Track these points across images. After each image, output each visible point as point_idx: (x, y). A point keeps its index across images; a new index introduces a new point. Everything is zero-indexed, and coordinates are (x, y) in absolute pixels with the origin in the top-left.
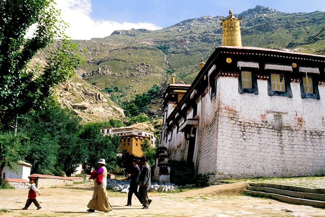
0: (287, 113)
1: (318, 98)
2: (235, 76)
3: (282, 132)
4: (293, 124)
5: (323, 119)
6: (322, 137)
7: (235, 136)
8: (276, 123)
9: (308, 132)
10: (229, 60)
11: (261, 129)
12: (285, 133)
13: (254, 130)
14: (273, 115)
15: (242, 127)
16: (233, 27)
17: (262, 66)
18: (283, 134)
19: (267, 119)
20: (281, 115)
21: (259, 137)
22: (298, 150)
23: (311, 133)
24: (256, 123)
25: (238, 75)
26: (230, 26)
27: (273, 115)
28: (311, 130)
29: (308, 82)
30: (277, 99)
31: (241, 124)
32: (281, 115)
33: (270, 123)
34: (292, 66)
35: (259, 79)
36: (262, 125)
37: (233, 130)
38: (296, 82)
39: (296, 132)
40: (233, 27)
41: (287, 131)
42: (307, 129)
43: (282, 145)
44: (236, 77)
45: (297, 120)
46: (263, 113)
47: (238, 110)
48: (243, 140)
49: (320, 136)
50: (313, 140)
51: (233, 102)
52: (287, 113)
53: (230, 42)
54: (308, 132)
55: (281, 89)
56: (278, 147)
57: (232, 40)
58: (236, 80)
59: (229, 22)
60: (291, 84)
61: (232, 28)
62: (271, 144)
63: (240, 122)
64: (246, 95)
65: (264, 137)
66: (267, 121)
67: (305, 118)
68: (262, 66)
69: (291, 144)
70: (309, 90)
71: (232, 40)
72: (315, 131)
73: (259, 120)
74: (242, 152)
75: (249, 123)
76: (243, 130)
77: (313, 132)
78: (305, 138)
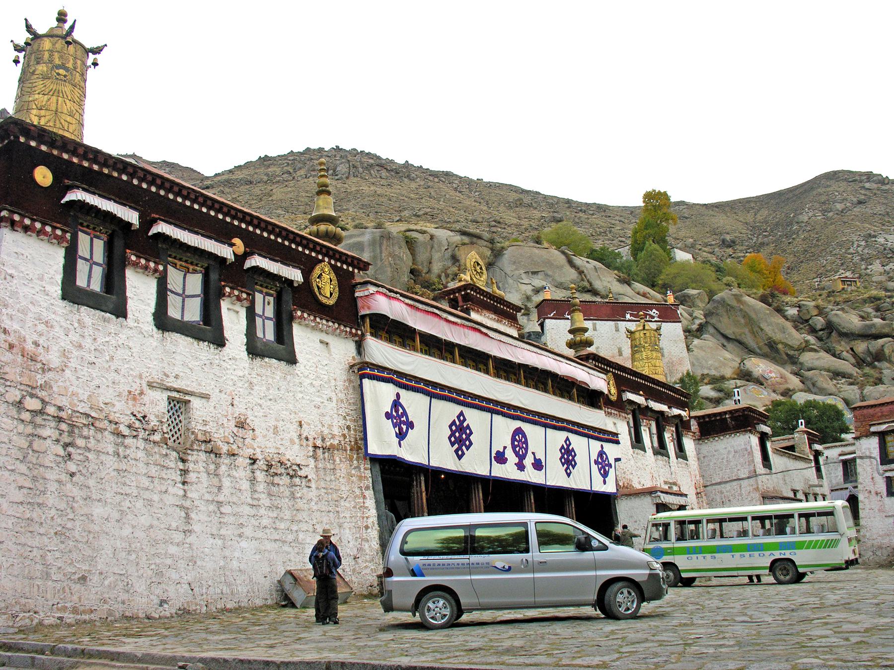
0: (205, 397)
1: (292, 360)
2: (56, 237)
3: (190, 458)
4: (221, 434)
5: (301, 426)
6: (297, 480)
7: (37, 459)
8: (177, 424)
9: (261, 464)
10: (43, 176)
11: (128, 441)
12: (198, 460)
13: (108, 442)
14: (165, 395)
15: (64, 426)
16: (67, 69)
17: (147, 222)
18: (191, 466)
19: (146, 410)
20: (187, 402)
21: (118, 470)
22: (232, 519)
23: (270, 466)
24: (111, 418)
25: (68, 236)
26: (57, 61)
27: (165, 395)
28: (269, 459)
29: (265, 305)
30: (182, 343)
31: (63, 414)
32: (187, 402)
33: (154, 422)
34: (232, 245)
35: (135, 265)
36: (129, 426)
37: (33, 435)
38: (239, 299)
39: (227, 460)
40: (67, 69)
41: (203, 456)
42: (259, 456)
43: (188, 504)
44: (60, 240)
45: (232, 423)
46: (136, 389)
47: (53, 358)
48: (64, 477)
49: (292, 477)
50: (274, 489)
51: (41, 327)
52: (205, 397)
53: (47, 118)
54: (261, 464)
55: (193, 313)
56: (178, 510)
57: (57, 111)
58: (58, 256)
59: (57, 46)
60: (222, 302)
61: (61, 71)
62: (156, 498)
63: (60, 409)
64: (87, 315)
65: (134, 470)
66: (144, 417)
67: (254, 420)
68: (147, 222)
69: (213, 501)
70: (267, 332)
71: (57, 111)
72: (279, 462)
73: (121, 411)
74: (59, 521)
75: (88, 416)
76: (66, 439)
77: (273, 463)
78: (253, 480)
